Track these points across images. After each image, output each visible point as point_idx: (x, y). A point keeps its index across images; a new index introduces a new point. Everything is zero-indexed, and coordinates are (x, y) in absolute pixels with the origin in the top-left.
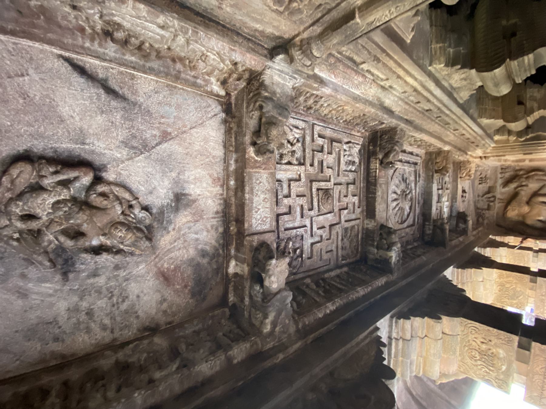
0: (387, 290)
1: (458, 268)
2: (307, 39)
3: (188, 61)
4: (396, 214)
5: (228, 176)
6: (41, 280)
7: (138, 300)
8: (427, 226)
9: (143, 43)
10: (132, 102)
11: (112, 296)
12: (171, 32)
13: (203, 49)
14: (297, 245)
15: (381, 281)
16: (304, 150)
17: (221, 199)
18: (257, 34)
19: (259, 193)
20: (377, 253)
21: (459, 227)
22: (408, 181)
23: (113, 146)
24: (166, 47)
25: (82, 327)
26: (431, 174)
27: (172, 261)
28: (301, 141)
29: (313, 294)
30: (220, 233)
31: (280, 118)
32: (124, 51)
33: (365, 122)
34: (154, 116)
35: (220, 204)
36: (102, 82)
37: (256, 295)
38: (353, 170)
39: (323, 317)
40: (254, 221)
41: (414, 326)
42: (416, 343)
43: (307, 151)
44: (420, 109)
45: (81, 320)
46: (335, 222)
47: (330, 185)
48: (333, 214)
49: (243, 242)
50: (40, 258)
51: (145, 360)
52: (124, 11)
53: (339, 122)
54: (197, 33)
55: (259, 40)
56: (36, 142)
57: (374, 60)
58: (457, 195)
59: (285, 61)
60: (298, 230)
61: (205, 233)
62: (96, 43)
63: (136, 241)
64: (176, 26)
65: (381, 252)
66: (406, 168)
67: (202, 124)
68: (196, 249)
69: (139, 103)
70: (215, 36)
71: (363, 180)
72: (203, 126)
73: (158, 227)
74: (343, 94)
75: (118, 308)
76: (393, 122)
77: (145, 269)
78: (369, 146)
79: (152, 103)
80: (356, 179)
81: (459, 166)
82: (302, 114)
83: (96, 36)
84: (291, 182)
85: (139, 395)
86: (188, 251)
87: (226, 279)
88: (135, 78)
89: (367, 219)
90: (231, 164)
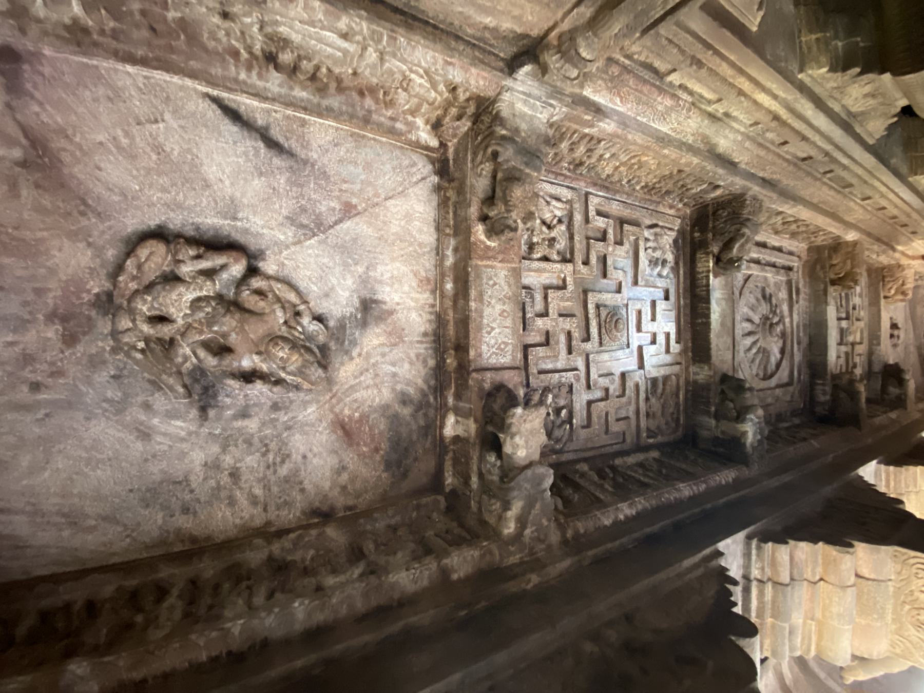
1: (888, 463)
2: (569, 31)
3: (382, 92)
4: (753, 361)
5: (443, 275)
6: (171, 415)
7: (305, 464)
8: (820, 387)
9: (317, 68)
10: (302, 159)
11: (268, 451)
12: (358, 43)
13: (405, 67)
14: (562, 402)
15: (726, 476)
16: (571, 238)
17: (431, 313)
18: (487, 35)
20: (717, 427)
22: (774, 301)
23: (274, 223)
24: (350, 71)
25: (223, 494)
26: (822, 286)
27: (356, 405)
28: (566, 223)
29: (592, 488)
30: (430, 369)
31: (527, 171)
32: (292, 83)
33: (683, 186)
34: (332, 179)
35: (430, 321)
36: (262, 131)
37: (489, 472)
41: (796, 559)
42: (802, 592)
43: (576, 238)
44: (787, 157)
45: (222, 483)
49: (467, 381)
50: (171, 381)
51: (312, 559)
52: (292, 14)
53: (634, 189)
54: (395, 39)
55: (491, 45)
56: (172, 215)
57: (691, 65)
58: (880, 330)
59: (533, 75)
60: (564, 374)
61: (407, 366)
62: (254, 73)
63: (303, 366)
64: (365, 31)
65: (725, 426)
66: (769, 275)
68: (394, 390)
69: (311, 161)
70: (422, 41)
71: (684, 294)
72: (405, 196)
73: (337, 349)
74: (638, 131)
75: (275, 472)
76: (737, 183)
77: (316, 414)
78: (692, 232)
79: (329, 162)
81: (881, 276)
83: (254, 62)
84: (550, 291)
85: (300, 605)
86: (380, 391)
87: (441, 446)
88: (306, 123)
89: (694, 364)
90: (448, 256)
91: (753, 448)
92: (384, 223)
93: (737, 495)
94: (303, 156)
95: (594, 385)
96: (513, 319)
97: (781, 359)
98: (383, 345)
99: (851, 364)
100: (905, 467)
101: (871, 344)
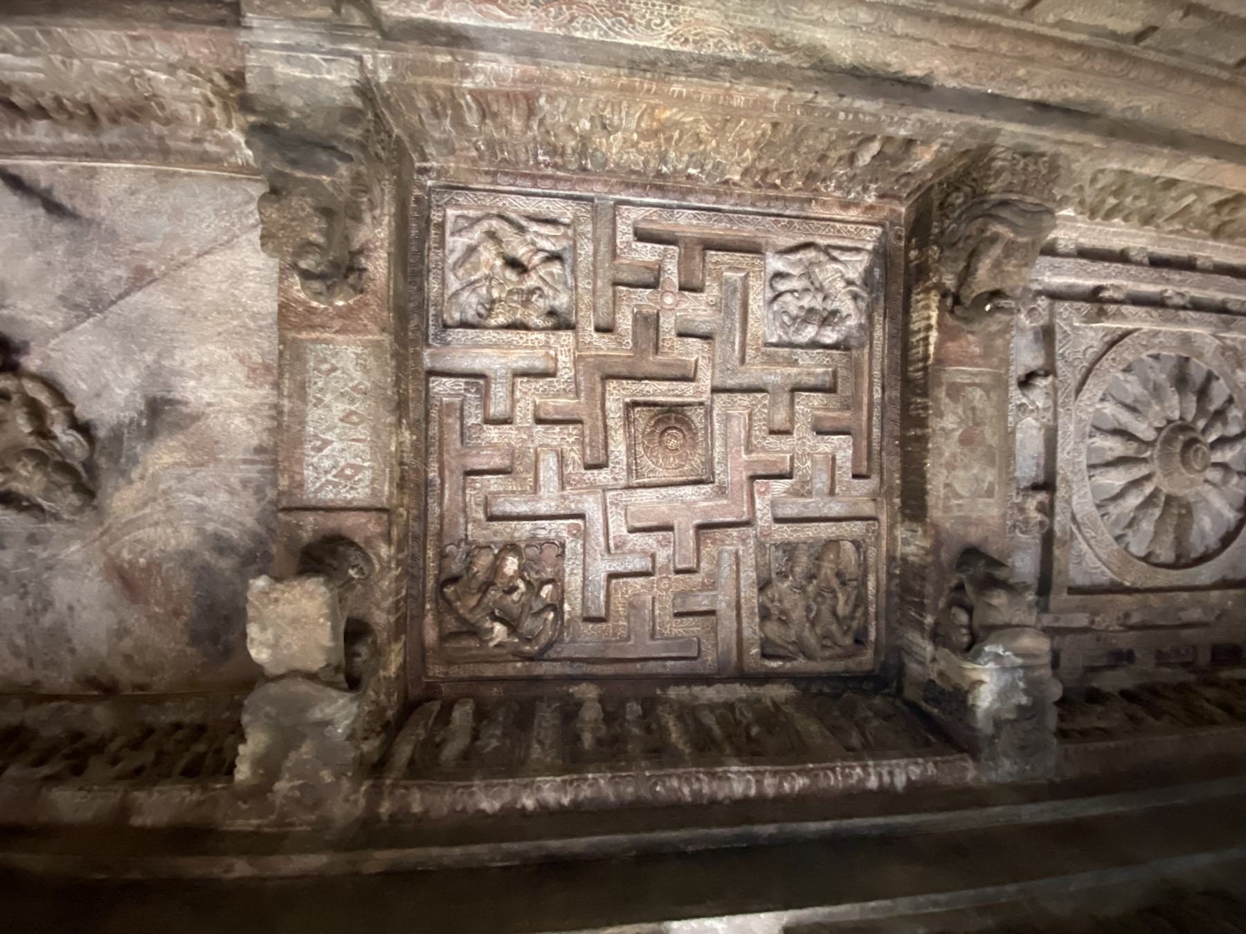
0: (886, 813)
7: (71, 616)
11: (26, 593)
15: (902, 772)
17: (273, 418)
19: (328, 398)
20: (934, 660)
27: (139, 547)
31: (300, 174)
38: (828, 341)
39: (494, 815)
40: (309, 473)
60: (545, 523)
61: (223, 497)
67: (228, 242)
68: (200, 530)
72: (232, 248)
75: (37, 621)
76: (952, 127)
78: (907, 249)
80: (841, 372)
82: (559, 179)
86: (176, 531)
92: (193, 289)
93: (880, 820)
94: (88, 216)
95: (617, 547)
96: (374, 428)
98: (180, 464)
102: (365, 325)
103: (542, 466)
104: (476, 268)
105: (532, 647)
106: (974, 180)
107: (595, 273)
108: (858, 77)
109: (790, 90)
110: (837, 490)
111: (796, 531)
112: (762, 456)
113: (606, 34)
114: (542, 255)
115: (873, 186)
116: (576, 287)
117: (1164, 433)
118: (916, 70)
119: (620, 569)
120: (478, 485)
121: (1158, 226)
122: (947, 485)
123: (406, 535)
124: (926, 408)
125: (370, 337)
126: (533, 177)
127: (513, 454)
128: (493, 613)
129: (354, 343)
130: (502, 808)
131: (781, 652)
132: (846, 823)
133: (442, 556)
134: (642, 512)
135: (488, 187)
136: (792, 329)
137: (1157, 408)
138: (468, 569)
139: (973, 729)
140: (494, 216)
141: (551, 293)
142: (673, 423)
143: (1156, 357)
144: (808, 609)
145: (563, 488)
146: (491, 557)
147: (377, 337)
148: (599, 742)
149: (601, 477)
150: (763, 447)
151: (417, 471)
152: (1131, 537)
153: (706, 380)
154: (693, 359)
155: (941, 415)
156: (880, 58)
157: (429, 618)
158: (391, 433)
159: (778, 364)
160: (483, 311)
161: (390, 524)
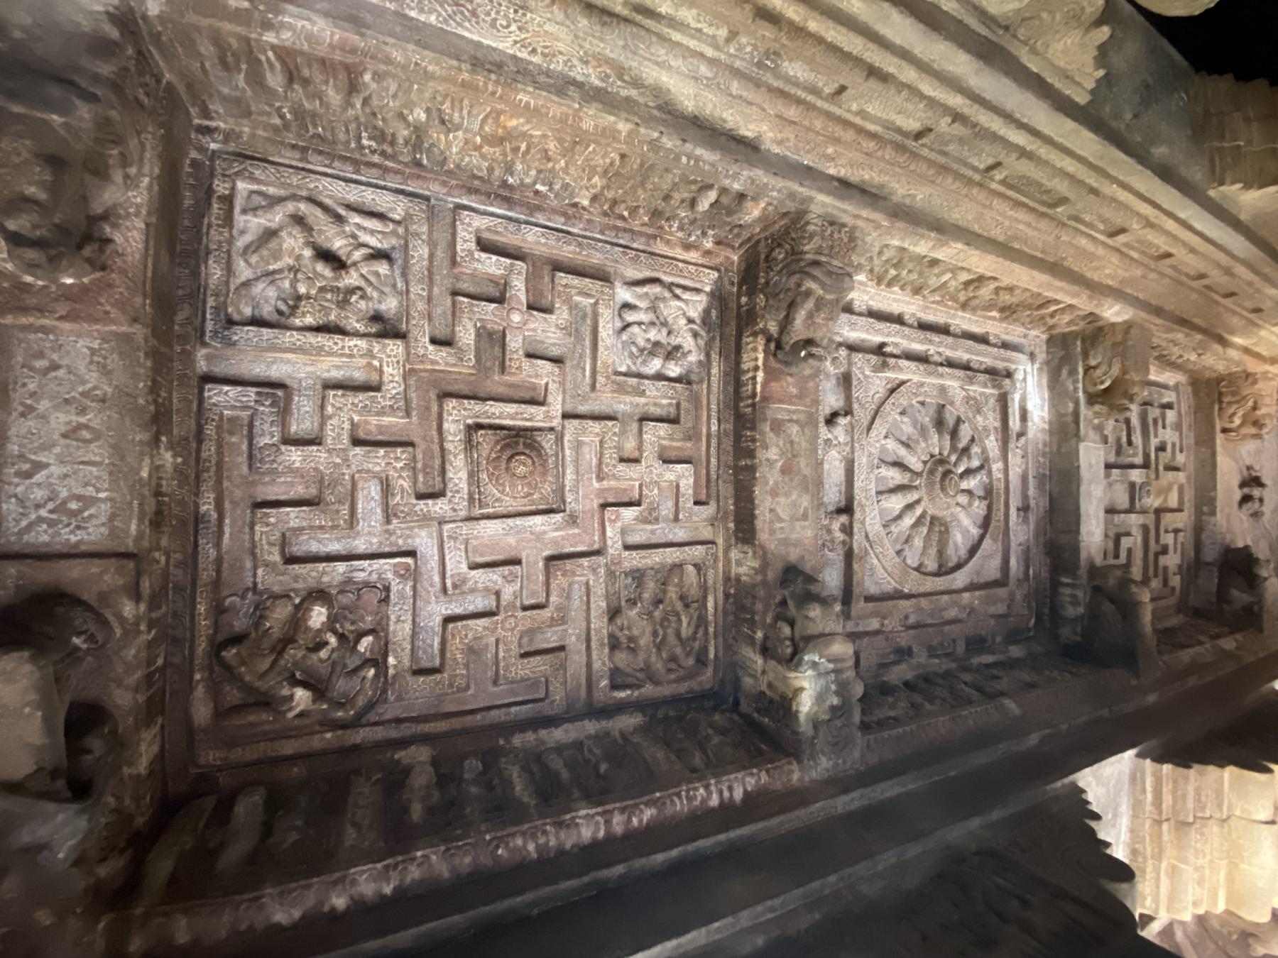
0: (726, 829)
1: (1159, 759)
8: (1068, 591)
20: (764, 672)
21: (1229, 602)
22: (965, 432)
38: (672, 375)
39: (295, 926)
46: (580, 548)
47: (533, 416)
48: (558, 517)
60: (365, 563)
80: (684, 404)
91: (816, 725)
93: (722, 837)
95: (455, 586)
97: (982, 537)
99: (1153, 546)
100: (1196, 767)
101: (1199, 513)
102: (107, 313)
103: (360, 496)
104: (277, 256)
105: (347, 711)
106: (793, 239)
107: (431, 280)
108: (699, 126)
109: (637, 124)
110: (681, 516)
111: (644, 558)
112: (613, 483)
113: (445, 21)
114: (364, 251)
115: (711, 232)
116: (408, 291)
117: (928, 465)
118: (748, 131)
119: (459, 611)
120: (272, 520)
121: (924, 297)
122: (771, 510)
123: (164, 588)
124: (754, 440)
125: (114, 328)
126: (355, 162)
127: (321, 481)
128: (294, 675)
129: (89, 334)
130: (303, 917)
131: (630, 680)
132: (691, 847)
133: (219, 610)
134: (486, 545)
135: (294, 163)
136: (640, 360)
137: (923, 445)
138: (257, 625)
139: (795, 733)
140: (302, 198)
141: (375, 294)
142: (521, 448)
143: (922, 403)
144: (655, 634)
145: (388, 522)
146: (290, 608)
147: (124, 329)
148: (430, 811)
149: (437, 508)
150: (614, 475)
151: (182, 503)
152: (907, 553)
153: (556, 405)
154: (543, 382)
155: (766, 447)
156: (717, 113)
157: (200, 691)
158: (142, 454)
159: (627, 393)
160: (284, 308)
161: (139, 574)
